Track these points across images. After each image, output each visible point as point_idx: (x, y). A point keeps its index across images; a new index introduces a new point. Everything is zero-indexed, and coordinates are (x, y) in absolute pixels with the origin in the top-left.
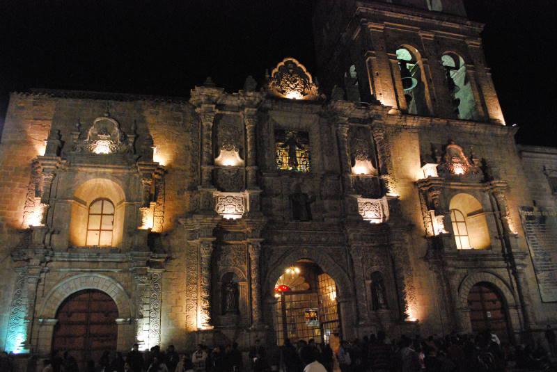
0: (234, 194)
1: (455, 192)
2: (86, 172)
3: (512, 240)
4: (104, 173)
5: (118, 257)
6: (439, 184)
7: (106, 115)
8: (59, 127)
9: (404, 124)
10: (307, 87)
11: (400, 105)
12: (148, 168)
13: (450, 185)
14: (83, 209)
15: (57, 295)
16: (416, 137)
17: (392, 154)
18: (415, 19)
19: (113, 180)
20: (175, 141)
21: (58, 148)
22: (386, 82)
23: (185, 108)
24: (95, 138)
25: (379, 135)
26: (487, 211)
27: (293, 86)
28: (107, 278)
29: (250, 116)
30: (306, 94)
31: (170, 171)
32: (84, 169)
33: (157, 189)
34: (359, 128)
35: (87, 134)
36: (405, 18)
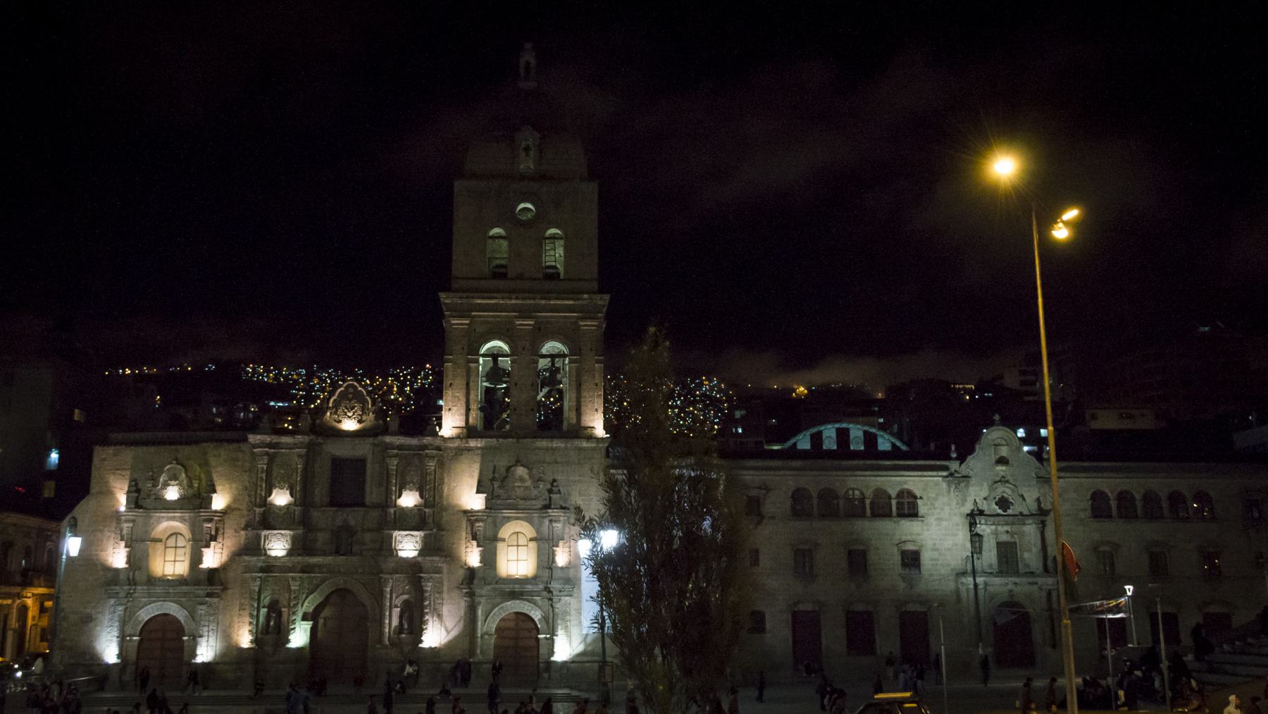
0: (283, 532)
1: (509, 519)
2: (159, 516)
3: (557, 574)
4: (174, 517)
5: (185, 588)
6: (482, 516)
7: (174, 462)
8: (136, 476)
9: (467, 445)
10: (366, 413)
11: (471, 420)
12: (206, 514)
13: (503, 513)
14: (160, 546)
15: (140, 619)
16: (478, 459)
17: (446, 481)
18: (514, 302)
19: (180, 522)
20: (235, 481)
21: (136, 501)
22: (458, 394)
23: (244, 447)
24: (166, 485)
25: (432, 465)
26: (541, 539)
27: (350, 414)
28: (176, 605)
29: (300, 456)
30: (364, 421)
31: (228, 511)
32: (158, 515)
33: (217, 530)
34: (415, 454)
35: (159, 481)
36: (501, 302)
